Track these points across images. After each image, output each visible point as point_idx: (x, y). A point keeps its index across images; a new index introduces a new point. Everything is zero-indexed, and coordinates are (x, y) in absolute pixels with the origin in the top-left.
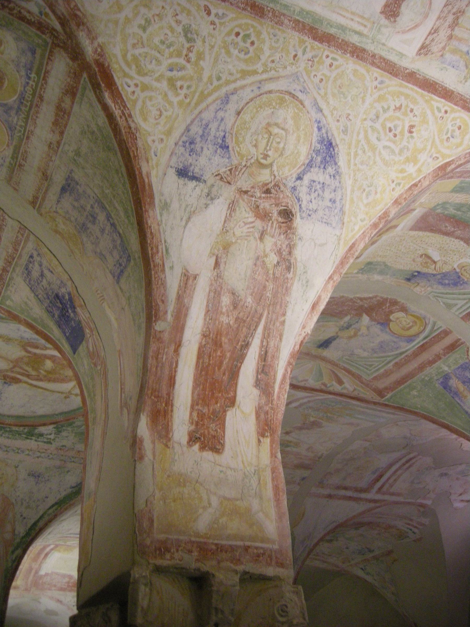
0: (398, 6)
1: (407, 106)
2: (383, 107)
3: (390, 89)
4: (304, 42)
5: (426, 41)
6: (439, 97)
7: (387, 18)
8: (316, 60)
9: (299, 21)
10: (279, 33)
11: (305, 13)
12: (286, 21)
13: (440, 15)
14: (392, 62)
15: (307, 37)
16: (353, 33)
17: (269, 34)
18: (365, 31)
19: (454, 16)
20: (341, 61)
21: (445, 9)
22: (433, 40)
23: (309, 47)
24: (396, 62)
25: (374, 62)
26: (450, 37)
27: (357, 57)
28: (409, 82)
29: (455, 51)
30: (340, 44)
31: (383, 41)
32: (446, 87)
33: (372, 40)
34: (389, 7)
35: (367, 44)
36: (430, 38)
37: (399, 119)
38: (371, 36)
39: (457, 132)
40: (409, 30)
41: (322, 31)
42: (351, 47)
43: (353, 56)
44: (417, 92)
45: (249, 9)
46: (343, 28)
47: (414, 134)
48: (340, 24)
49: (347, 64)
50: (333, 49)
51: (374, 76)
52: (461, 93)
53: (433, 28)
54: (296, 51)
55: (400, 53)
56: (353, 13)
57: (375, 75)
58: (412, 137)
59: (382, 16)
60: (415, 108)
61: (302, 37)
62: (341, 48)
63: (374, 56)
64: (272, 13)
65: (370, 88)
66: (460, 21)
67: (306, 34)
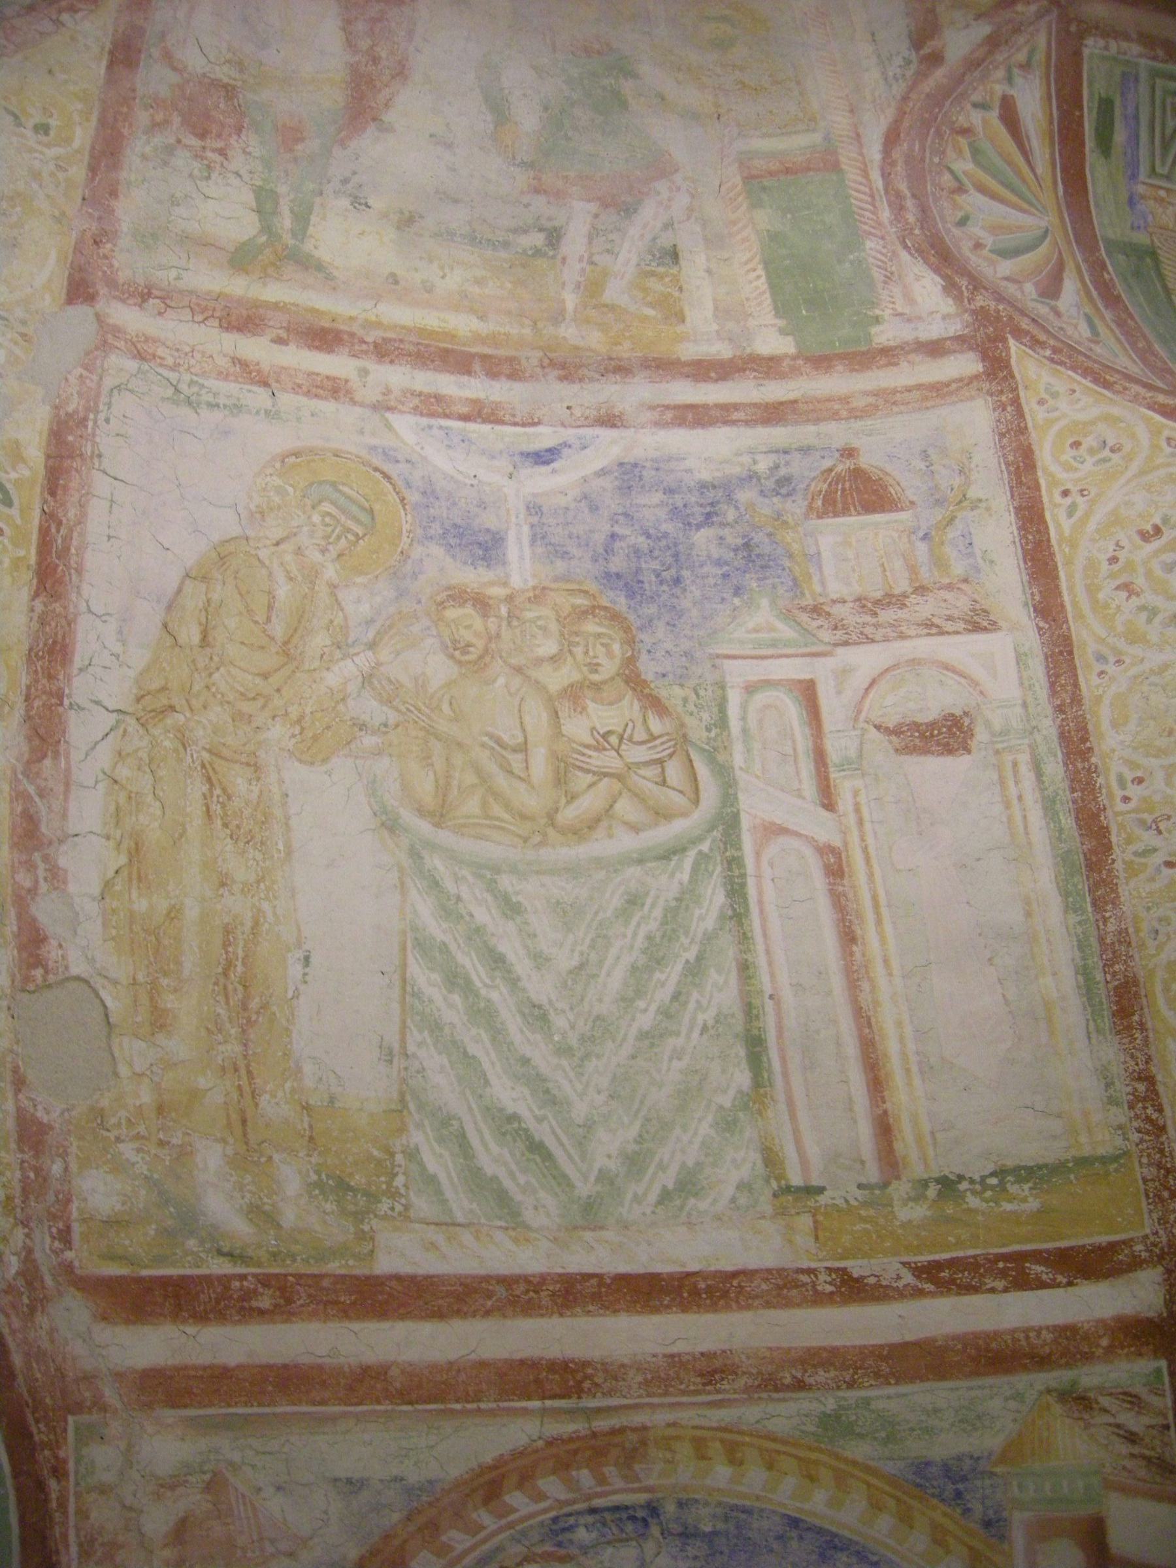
0: (933, 729)
1: (1112, 576)
2: (1149, 621)
3: (1102, 633)
4: (1128, 865)
5: (960, 630)
6: (1047, 528)
7: (969, 733)
8: (1148, 818)
9: (1094, 904)
10: (1145, 926)
11: (1071, 899)
12: (1112, 927)
13: (895, 639)
14: (1047, 667)
15: (1115, 865)
16: (1044, 779)
17: (1160, 948)
18: (1024, 758)
19: (878, 611)
20: (1116, 767)
21: (878, 638)
22: (949, 618)
23: (1132, 848)
24: (1042, 658)
25: (1072, 702)
26: (921, 590)
27: (1084, 740)
28: (1063, 606)
29: (940, 563)
30: (1083, 791)
31: (1019, 710)
32: (1019, 529)
33: (1031, 733)
34: (948, 744)
35: (1045, 738)
36: (949, 626)
37: (1149, 574)
38: (1026, 741)
39: (1089, 441)
40: (961, 674)
41: (1082, 844)
42: (1074, 765)
43: (1090, 749)
44: (1070, 577)
45: (1136, 1018)
46: (1049, 806)
47: (1157, 520)
48: (1046, 815)
49: (1113, 751)
50: (1103, 799)
51: (1099, 681)
52: (1008, 494)
53: (929, 634)
54: (1158, 871)
55: (1018, 663)
56: (1007, 805)
57: (1095, 680)
58: (1165, 520)
59: (973, 744)
60: (1104, 557)
61: (1122, 875)
62: (1088, 783)
63: (1060, 709)
64: (1112, 966)
65: (1130, 673)
66: (878, 595)
67: (1110, 871)
